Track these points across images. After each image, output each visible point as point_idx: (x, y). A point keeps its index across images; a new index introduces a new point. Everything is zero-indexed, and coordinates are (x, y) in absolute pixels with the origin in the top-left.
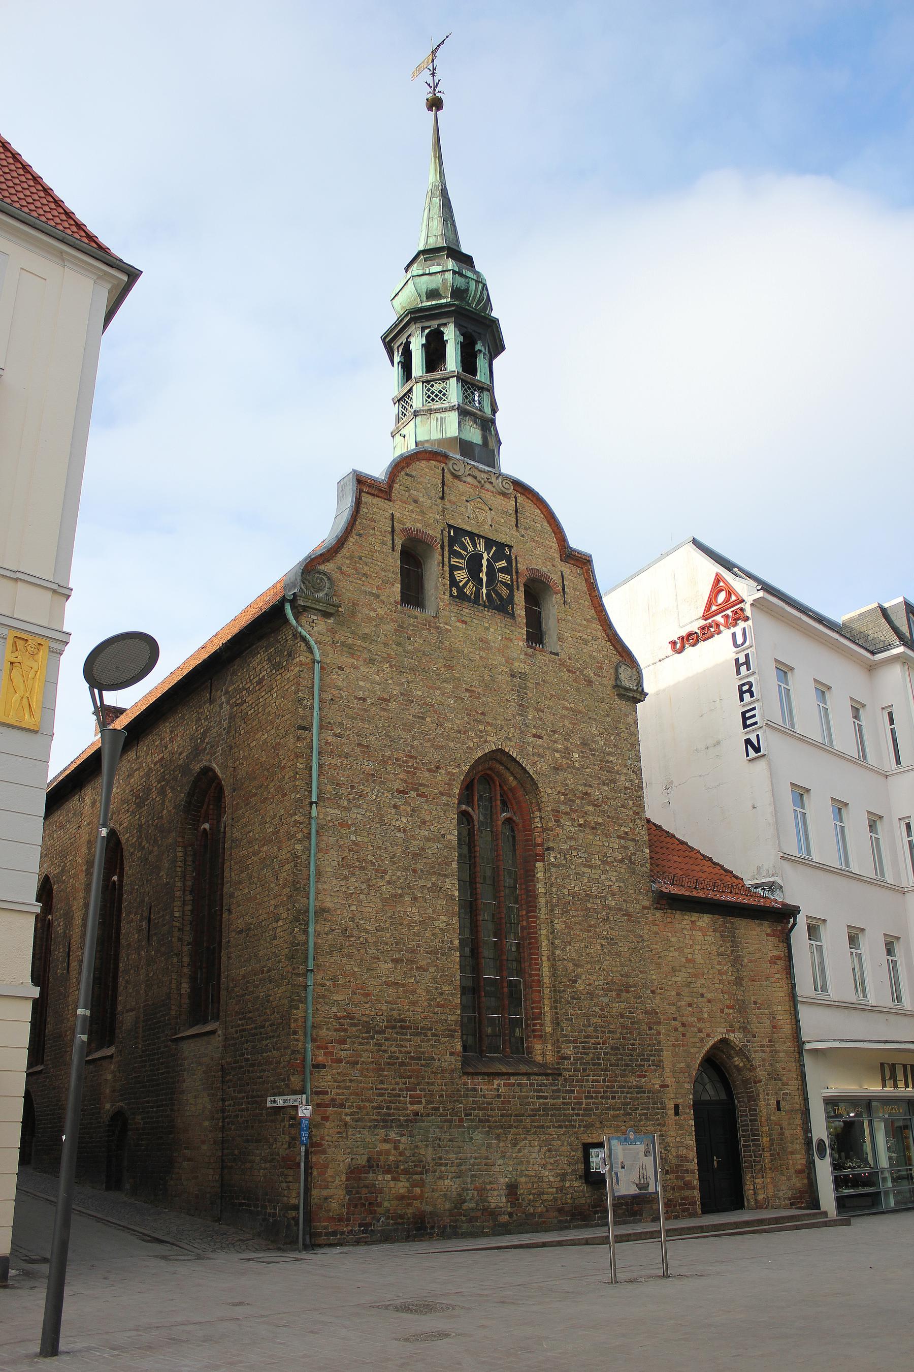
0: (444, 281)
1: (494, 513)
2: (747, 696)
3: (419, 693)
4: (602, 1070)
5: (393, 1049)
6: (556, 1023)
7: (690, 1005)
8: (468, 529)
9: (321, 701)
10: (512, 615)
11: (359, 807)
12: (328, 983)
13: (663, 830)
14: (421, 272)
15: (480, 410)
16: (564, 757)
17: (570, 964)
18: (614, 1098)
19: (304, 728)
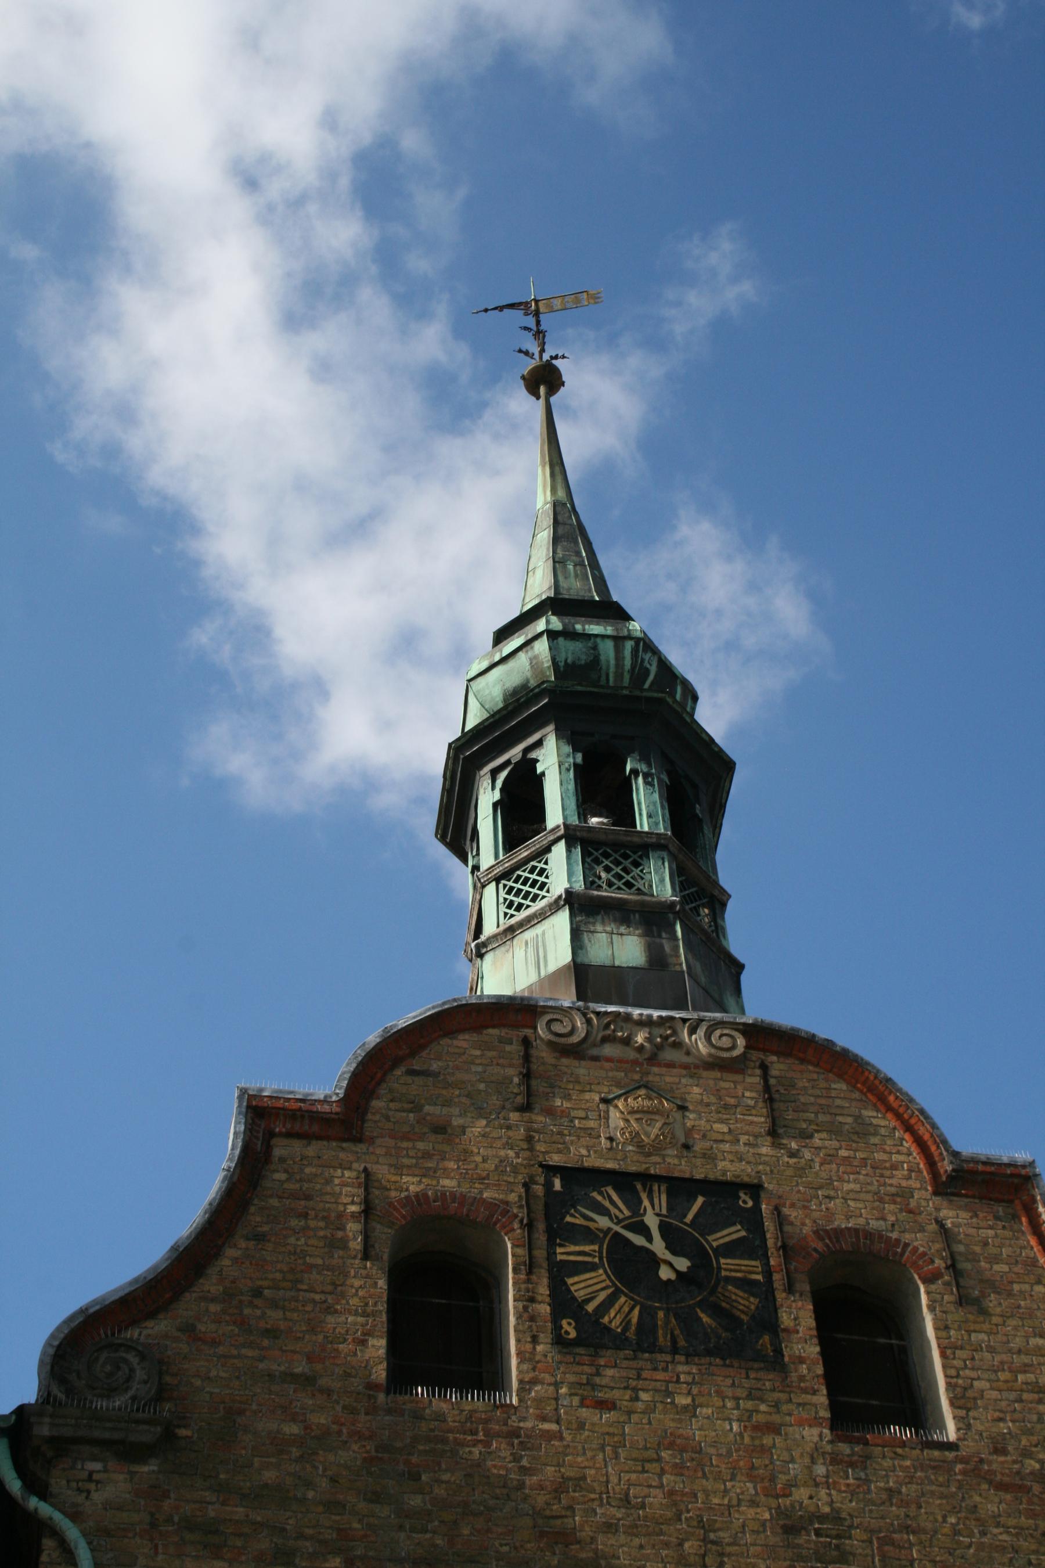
10: (776, 1362)
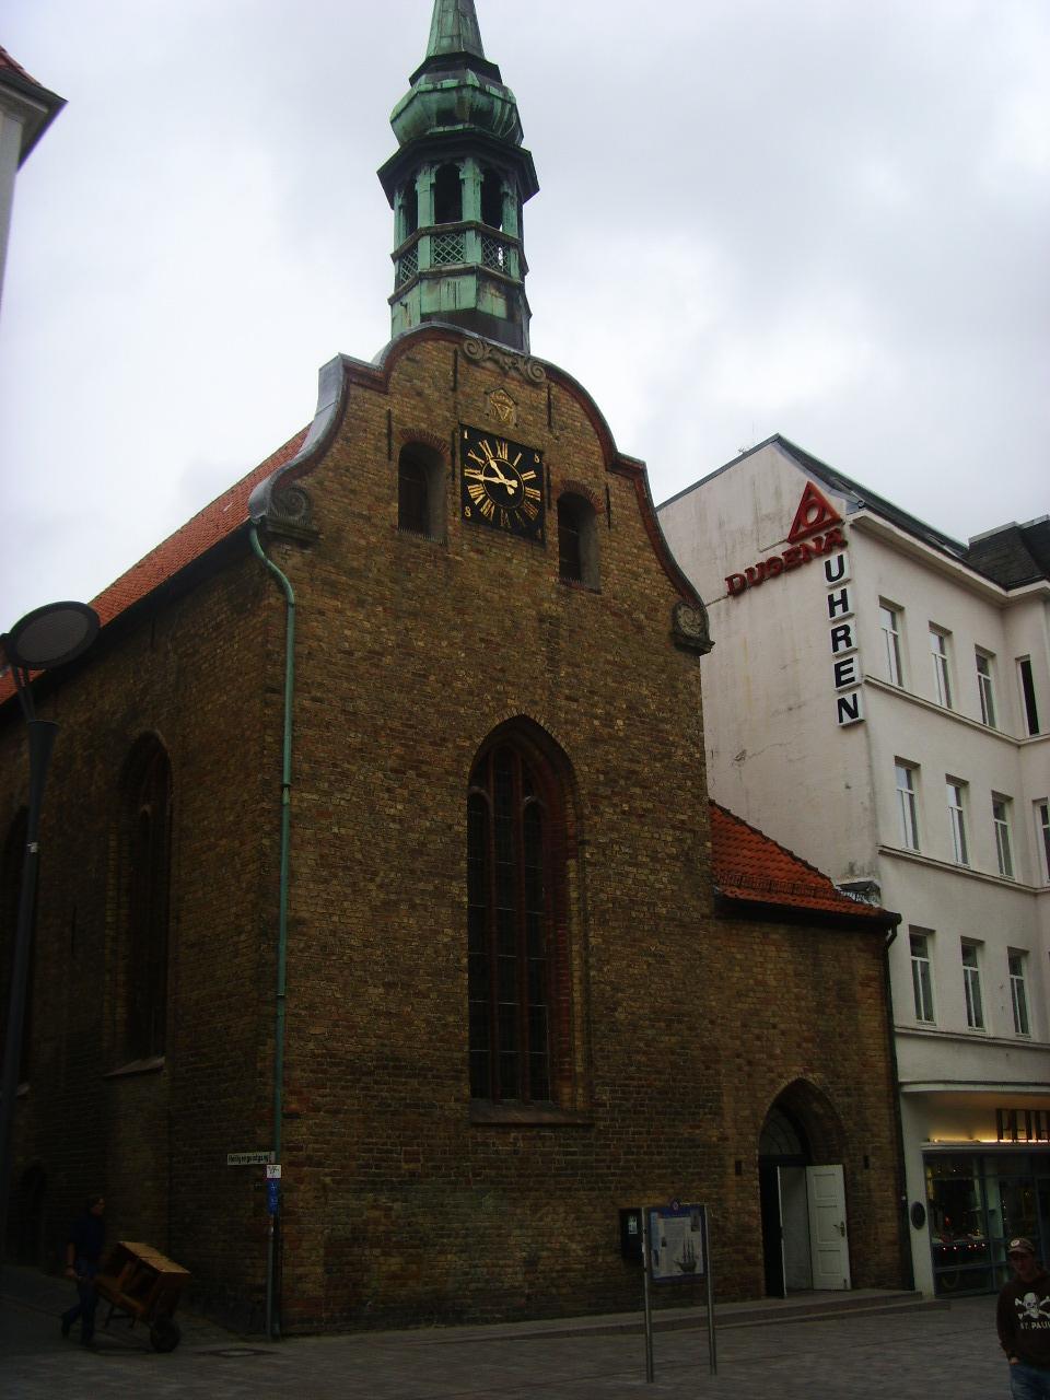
0: (461, 100)
1: (520, 409)
2: (842, 644)
3: (421, 644)
4: (645, 1119)
5: (384, 1094)
6: (590, 1061)
7: (758, 1038)
8: (487, 429)
9: (297, 656)
10: (542, 542)
11: (342, 791)
12: (303, 1013)
13: (732, 816)
14: (430, 87)
15: (505, 272)
16: (605, 726)
17: (608, 988)
18: (659, 1153)
19: (273, 691)
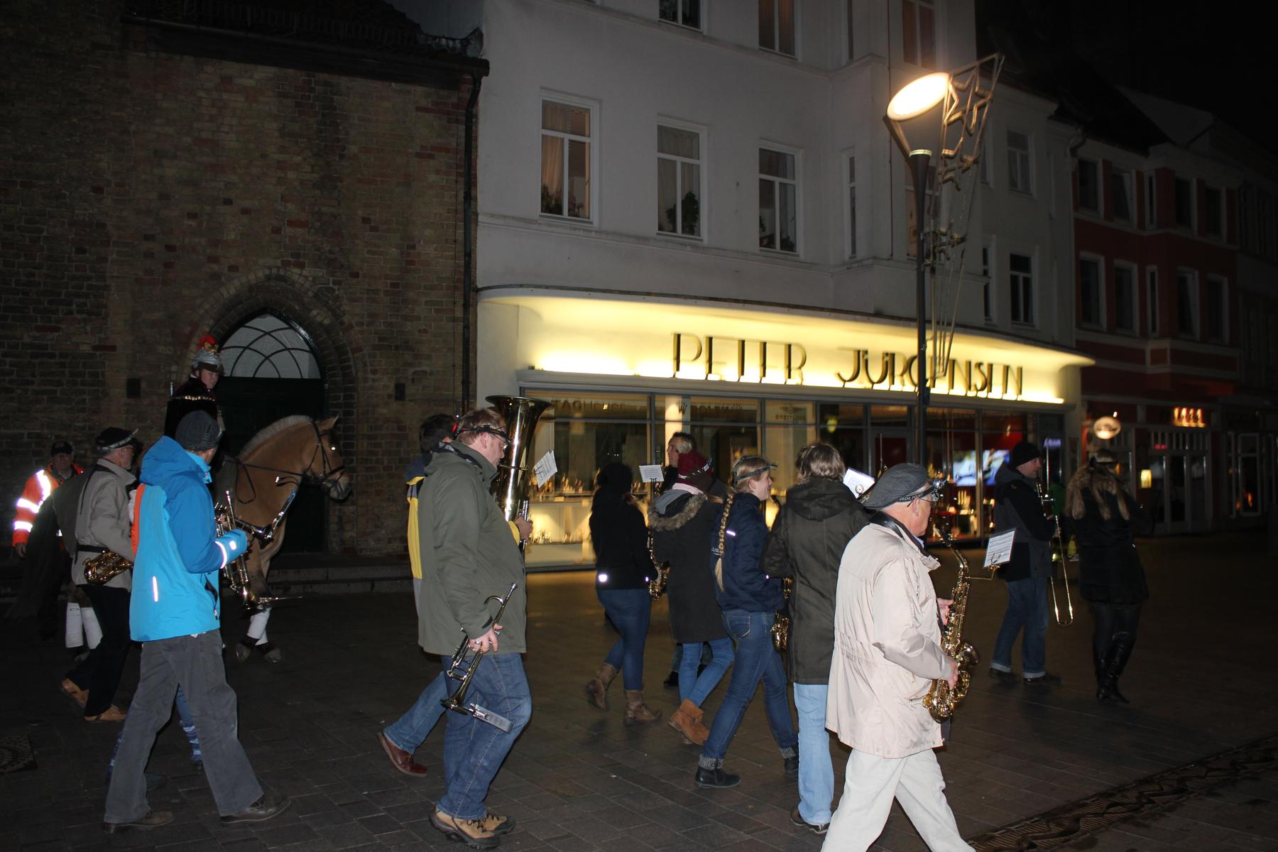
7: (192, 216)
